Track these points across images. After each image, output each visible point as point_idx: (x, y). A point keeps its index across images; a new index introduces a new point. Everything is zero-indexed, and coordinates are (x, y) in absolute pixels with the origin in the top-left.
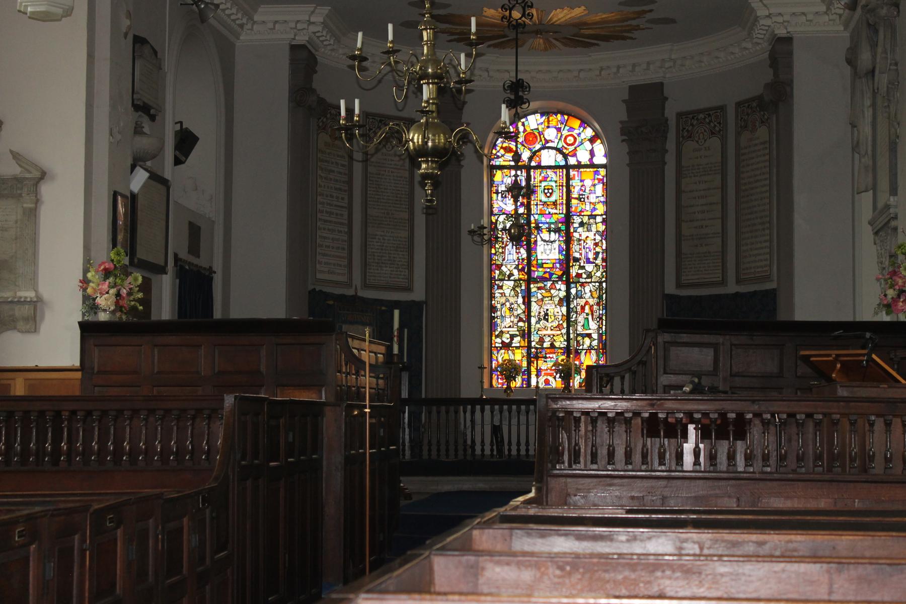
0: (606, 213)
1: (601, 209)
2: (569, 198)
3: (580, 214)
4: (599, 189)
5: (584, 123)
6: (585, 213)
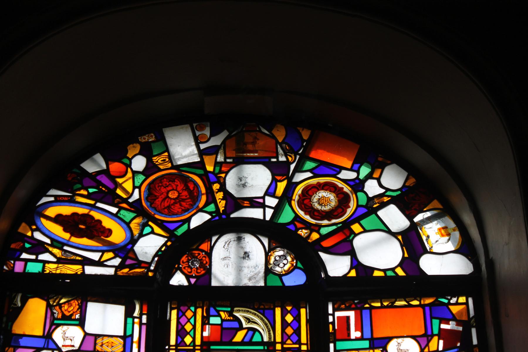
5: (376, 158)
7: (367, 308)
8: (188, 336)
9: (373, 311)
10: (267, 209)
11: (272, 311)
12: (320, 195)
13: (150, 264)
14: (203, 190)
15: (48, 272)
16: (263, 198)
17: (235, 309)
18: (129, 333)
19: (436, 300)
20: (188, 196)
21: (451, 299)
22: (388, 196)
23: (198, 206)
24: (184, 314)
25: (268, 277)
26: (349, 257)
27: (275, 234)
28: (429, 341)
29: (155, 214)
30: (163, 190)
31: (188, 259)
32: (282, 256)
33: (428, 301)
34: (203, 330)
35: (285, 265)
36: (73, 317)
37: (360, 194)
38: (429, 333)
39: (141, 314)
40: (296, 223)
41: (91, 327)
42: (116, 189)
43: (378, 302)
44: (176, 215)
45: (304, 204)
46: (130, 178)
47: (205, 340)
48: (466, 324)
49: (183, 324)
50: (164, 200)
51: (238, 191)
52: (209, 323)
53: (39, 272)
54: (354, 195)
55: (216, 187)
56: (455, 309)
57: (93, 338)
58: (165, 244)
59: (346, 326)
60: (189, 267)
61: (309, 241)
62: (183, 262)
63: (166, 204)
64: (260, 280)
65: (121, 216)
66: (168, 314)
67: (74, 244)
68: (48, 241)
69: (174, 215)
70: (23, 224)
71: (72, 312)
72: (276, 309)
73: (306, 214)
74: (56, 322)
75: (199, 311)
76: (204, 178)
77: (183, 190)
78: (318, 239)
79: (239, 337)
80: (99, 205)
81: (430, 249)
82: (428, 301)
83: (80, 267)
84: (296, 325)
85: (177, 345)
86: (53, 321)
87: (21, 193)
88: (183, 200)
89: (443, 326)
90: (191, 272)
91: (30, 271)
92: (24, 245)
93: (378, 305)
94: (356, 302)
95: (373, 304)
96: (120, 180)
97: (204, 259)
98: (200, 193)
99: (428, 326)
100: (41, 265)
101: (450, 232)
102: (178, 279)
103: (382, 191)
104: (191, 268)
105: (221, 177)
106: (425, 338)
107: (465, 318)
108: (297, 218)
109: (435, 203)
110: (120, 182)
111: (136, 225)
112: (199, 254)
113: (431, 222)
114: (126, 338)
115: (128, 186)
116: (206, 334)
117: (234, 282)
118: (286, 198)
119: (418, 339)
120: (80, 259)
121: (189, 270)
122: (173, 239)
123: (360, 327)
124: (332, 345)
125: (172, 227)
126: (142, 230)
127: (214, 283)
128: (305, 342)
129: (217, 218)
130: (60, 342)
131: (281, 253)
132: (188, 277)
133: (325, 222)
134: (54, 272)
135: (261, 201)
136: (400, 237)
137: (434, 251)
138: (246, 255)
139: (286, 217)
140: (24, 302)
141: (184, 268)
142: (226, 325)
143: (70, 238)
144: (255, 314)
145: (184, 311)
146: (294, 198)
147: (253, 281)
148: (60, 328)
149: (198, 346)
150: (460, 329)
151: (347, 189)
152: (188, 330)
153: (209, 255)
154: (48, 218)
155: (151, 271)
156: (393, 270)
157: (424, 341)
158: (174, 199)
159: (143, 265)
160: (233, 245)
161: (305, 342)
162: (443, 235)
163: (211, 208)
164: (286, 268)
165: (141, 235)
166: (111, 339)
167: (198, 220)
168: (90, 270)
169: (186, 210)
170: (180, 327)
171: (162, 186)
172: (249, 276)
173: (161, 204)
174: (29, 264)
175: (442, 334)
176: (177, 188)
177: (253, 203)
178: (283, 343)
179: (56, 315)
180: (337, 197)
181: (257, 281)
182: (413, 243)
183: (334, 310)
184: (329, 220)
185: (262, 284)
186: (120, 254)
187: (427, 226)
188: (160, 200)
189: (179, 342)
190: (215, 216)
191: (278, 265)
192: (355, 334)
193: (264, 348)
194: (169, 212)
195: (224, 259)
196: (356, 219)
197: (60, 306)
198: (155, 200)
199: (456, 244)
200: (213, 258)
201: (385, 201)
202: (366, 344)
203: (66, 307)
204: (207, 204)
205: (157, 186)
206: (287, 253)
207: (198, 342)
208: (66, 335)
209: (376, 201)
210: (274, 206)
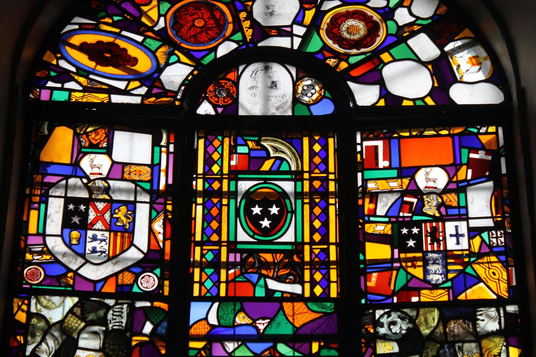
0: (517, 294)
1: (492, 281)
2: (353, 237)
3: (402, 302)
4: (480, 203)
6: (426, 296)
7: (395, 138)
8: (216, 165)
9: (402, 141)
10: (295, 38)
11: (300, 140)
12: (349, 23)
13: (176, 93)
14: (230, 19)
15: (74, 100)
16: (291, 26)
17: (263, 138)
18: (156, 161)
19: (466, 130)
20: (214, 25)
21: (481, 128)
22: (419, 25)
23: (224, 35)
24: (211, 143)
25: (296, 107)
26: (378, 86)
27: (303, 63)
28: (457, 171)
29: (181, 43)
30: (189, 18)
31: (215, 88)
32: (309, 85)
33: (458, 131)
34: (230, 159)
35: (313, 94)
36: (100, 146)
37: (390, 23)
38: (458, 162)
39: (168, 143)
40: (324, 52)
41: (119, 155)
42: (141, 18)
43: (406, 132)
44: (202, 43)
45: (332, 33)
46: (155, 6)
47: (232, 169)
48: (495, 154)
49: (211, 153)
50: (190, 28)
51: (265, 20)
52: (236, 153)
53: (66, 100)
54: (384, 24)
55: (243, 15)
56: (484, 139)
57: (120, 166)
58: (191, 73)
59: (374, 156)
60: (216, 96)
61: (338, 70)
62: (210, 92)
63: (192, 33)
64: (288, 109)
65: (147, 45)
66: (196, 144)
67: (99, 73)
68: (73, 69)
69: (200, 43)
70: (48, 53)
71: (99, 141)
72: (304, 138)
73: (334, 43)
74: (83, 150)
75: (227, 140)
76: (231, 6)
77: (209, 18)
78: (346, 68)
79: (267, 166)
80: (124, 33)
81: (461, 78)
82: (458, 131)
83: (107, 95)
84: (324, 154)
85: (204, 174)
86: (81, 149)
87: (45, 20)
88: (210, 29)
89: (472, 156)
90: (218, 102)
91: (56, 100)
92: (50, 73)
93: (407, 134)
94: (384, 131)
95: (402, 134)
96: (145, 8)
97: (231, 88)
98: (227, 22)
99: (456, 155)
100: (67, 93)
101: (481, 61)
102: (205, 109)
103: (413, 19)
104: (218, 98)
105: (248, 5)
106: (454, 168)
107: (494, 147)
108: (325, 47)
109: (467, 32)
110: (145, 10)
111: (162, 54)
112: (226, 83)
113: (462, 51)
114: (154, 166)
115: (153, 14)
116: (233, 163)
117: (262, 111)
118: (314, 27)
119: (446, 168)
120: (106, 87)
121: (216, 100)
122: (200, 68)
123: (388, 156)
124: (359, 175)
125: (198, 55)
126: (168, 59)
127: (241, 113)
128: (333, 171)
129: (244, 47)
130: (88, 170)
131: (309, 82)
132: (215, 107)
133: (354, 51)
134: (80, 100)
135: (289, 29)
136: (430, 67)
137: (464, 80)
138: (274, 85)
139: (314, 46)
140: (51, 130)
141: (211, 97)
142: (253, 154)
143: (96, 66)
144: (283, 144)
145: (211, 140)
146: (322, 27)
147: (281, 110)
148: (88, 156)
149: (225, 175)
150: (490, 158)
151: (376, 17)
152: (216, 160)
153: (236, 84)
154: (73, 46)
155: (178, 100)
156: (422, 99)
157: (452, 170)
158: (200, 27)
159: (169, 94)
160: (260, 74)
161: (333, 171)
162: (474, 65)
163: (238, 36)
164: (314, 97)
165: (167, 64)
166: (138, 168)
167: (225, 49)
168: (116, 99)
169: (213, 39)
170: (207, 156)
171: (188, 14)
172: (277, 105)
173: (187, 33)
174: (55, 92)
175: (471, 163)
176: (203, 16)
177: (281, 31)
178: (310, 172)
179: (83, 144)
180: (366, 26)
181: (285, 111)
182: (443, 72)
183: (363, 140)
184: (358, 49)
185: (290, 113)
186: (146, 83)
187: (458, 55)
188: (186, 28)
189: (206, 170)
190: (242, 45)
191: (306, 95)
192: (383, 163)
193: (292, 176)
194: (196, 41)
195: (252, 88)
196: (386, 48)
197: (87, 134)
198: (181, 28)
199: (488, 73)
200: (240, 87)
201: (416, 29)
202: (394, 173)
203: (93, 135)
204: (234, 33)
205: (182, 14)
206: (315, 82)
207: (226, 171)
208: (94, 164)
209: (406, 29)
210: (301, 34)
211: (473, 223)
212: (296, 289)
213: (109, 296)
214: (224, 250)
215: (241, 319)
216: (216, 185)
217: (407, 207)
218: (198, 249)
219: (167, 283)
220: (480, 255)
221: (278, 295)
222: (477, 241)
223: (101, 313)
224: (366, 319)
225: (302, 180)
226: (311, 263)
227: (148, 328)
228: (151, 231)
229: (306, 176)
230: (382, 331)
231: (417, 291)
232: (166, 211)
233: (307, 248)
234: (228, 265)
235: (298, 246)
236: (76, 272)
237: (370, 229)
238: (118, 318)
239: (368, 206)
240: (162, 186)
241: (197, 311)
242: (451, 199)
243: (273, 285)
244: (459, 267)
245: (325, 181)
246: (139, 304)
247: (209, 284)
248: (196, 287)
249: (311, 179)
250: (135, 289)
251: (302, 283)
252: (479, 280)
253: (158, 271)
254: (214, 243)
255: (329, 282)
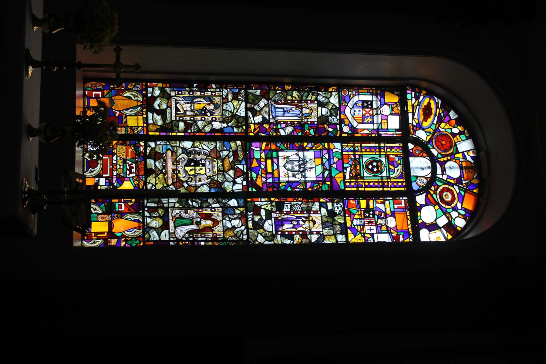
2: (367, 196)
3: (346, 211)
6: (348, 219)
178: (390, 182)
202: (392, 210)
207: (388, 153)
211: (375, 235)
212: (348, 177)
213: (340, 117)
214: (360, 153)
215: (336, 160)
216: (382, 150)
217: (380, 213)
218: (359, 145)
219: (346, 135)
220: (364, 237)
221: (345, 171)
222: (369, 236)
223: (334, 114)
224: (339, 200)
225: (387, 179)
226: (358, 182)
227: (330, 130)
228: (364, 129)
229: (389, 180)
230: (335, 204)
231: (350, 216)
232: (372, 134)
233: (363, 180)
234: (354, 155)
235: (363, 178)
236: (347, 106)
237: (371, 202)
238: (332, 120)
239: (379, 201)
240: (380, 133)
241: (338, 145)
242: (384, 228)
243: (348, 169)
244: (359, 230)
245: (388, 187)
246: (338, 126)
247: (347, 149)
248: (346, 145)
249: (388, 182)
250: (343, 125)
251: (350, 179)
252: (355, 236)
253: (350, 132)
254: (361, 150)
255: (351, 188)
